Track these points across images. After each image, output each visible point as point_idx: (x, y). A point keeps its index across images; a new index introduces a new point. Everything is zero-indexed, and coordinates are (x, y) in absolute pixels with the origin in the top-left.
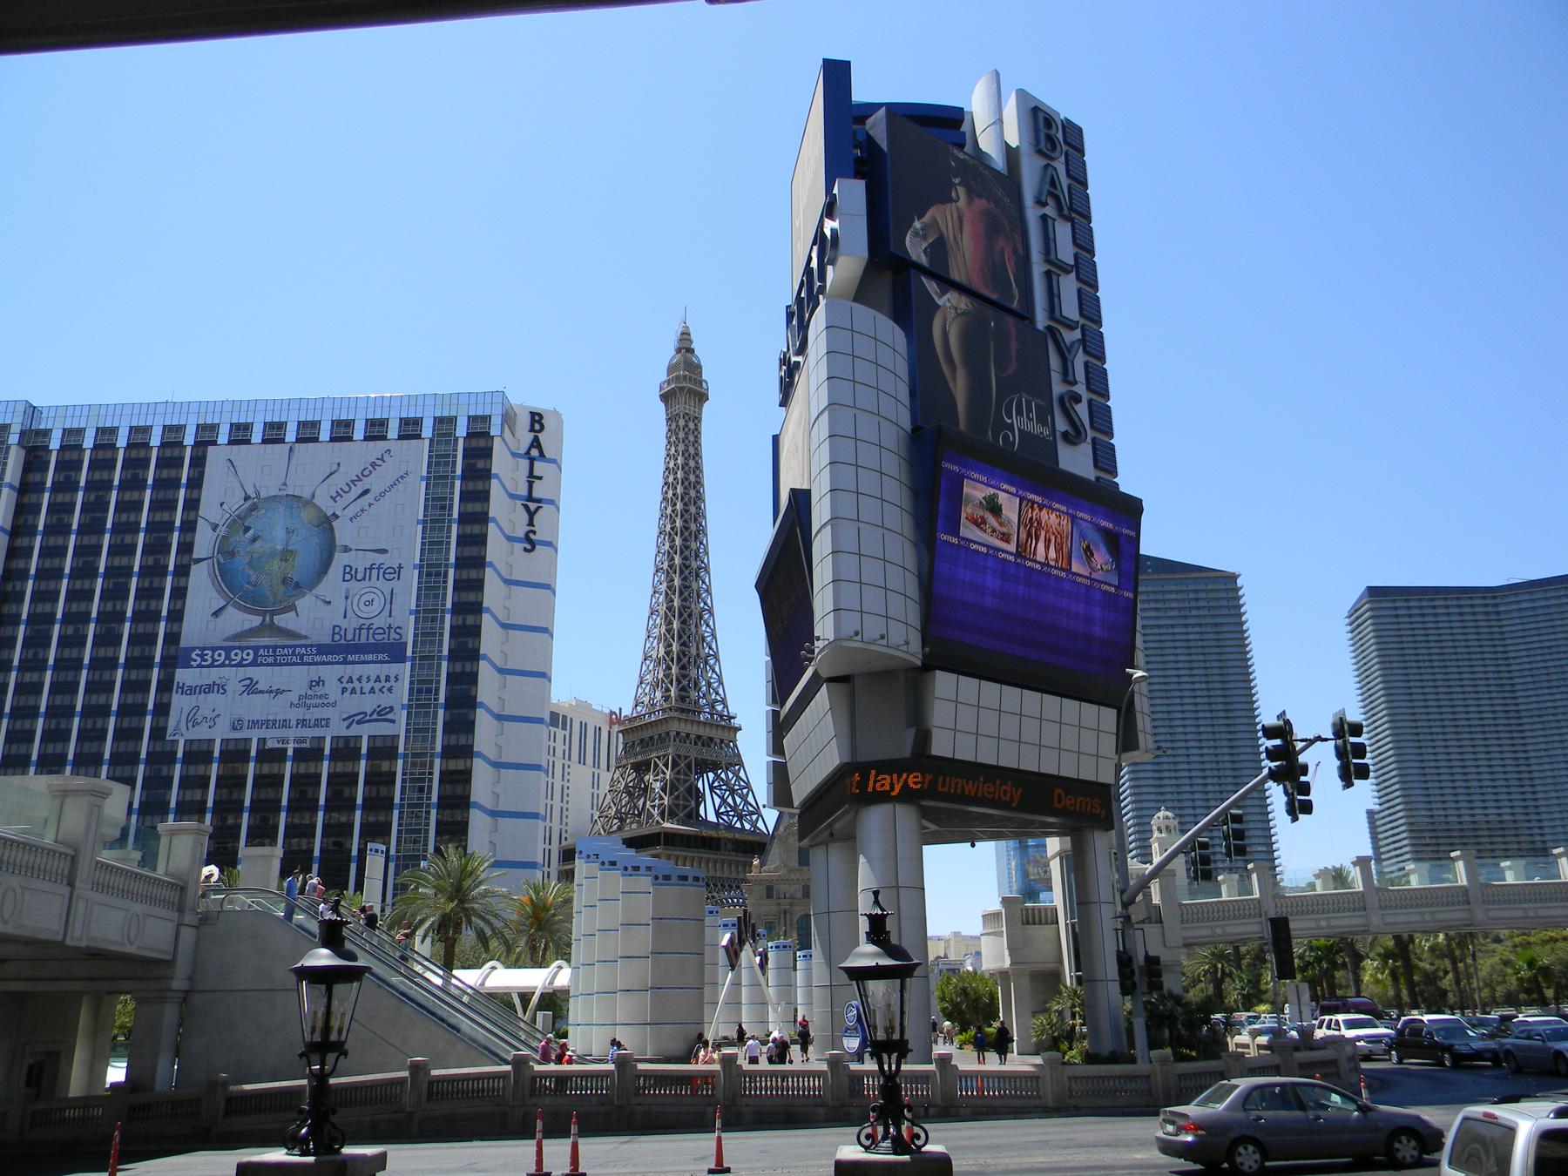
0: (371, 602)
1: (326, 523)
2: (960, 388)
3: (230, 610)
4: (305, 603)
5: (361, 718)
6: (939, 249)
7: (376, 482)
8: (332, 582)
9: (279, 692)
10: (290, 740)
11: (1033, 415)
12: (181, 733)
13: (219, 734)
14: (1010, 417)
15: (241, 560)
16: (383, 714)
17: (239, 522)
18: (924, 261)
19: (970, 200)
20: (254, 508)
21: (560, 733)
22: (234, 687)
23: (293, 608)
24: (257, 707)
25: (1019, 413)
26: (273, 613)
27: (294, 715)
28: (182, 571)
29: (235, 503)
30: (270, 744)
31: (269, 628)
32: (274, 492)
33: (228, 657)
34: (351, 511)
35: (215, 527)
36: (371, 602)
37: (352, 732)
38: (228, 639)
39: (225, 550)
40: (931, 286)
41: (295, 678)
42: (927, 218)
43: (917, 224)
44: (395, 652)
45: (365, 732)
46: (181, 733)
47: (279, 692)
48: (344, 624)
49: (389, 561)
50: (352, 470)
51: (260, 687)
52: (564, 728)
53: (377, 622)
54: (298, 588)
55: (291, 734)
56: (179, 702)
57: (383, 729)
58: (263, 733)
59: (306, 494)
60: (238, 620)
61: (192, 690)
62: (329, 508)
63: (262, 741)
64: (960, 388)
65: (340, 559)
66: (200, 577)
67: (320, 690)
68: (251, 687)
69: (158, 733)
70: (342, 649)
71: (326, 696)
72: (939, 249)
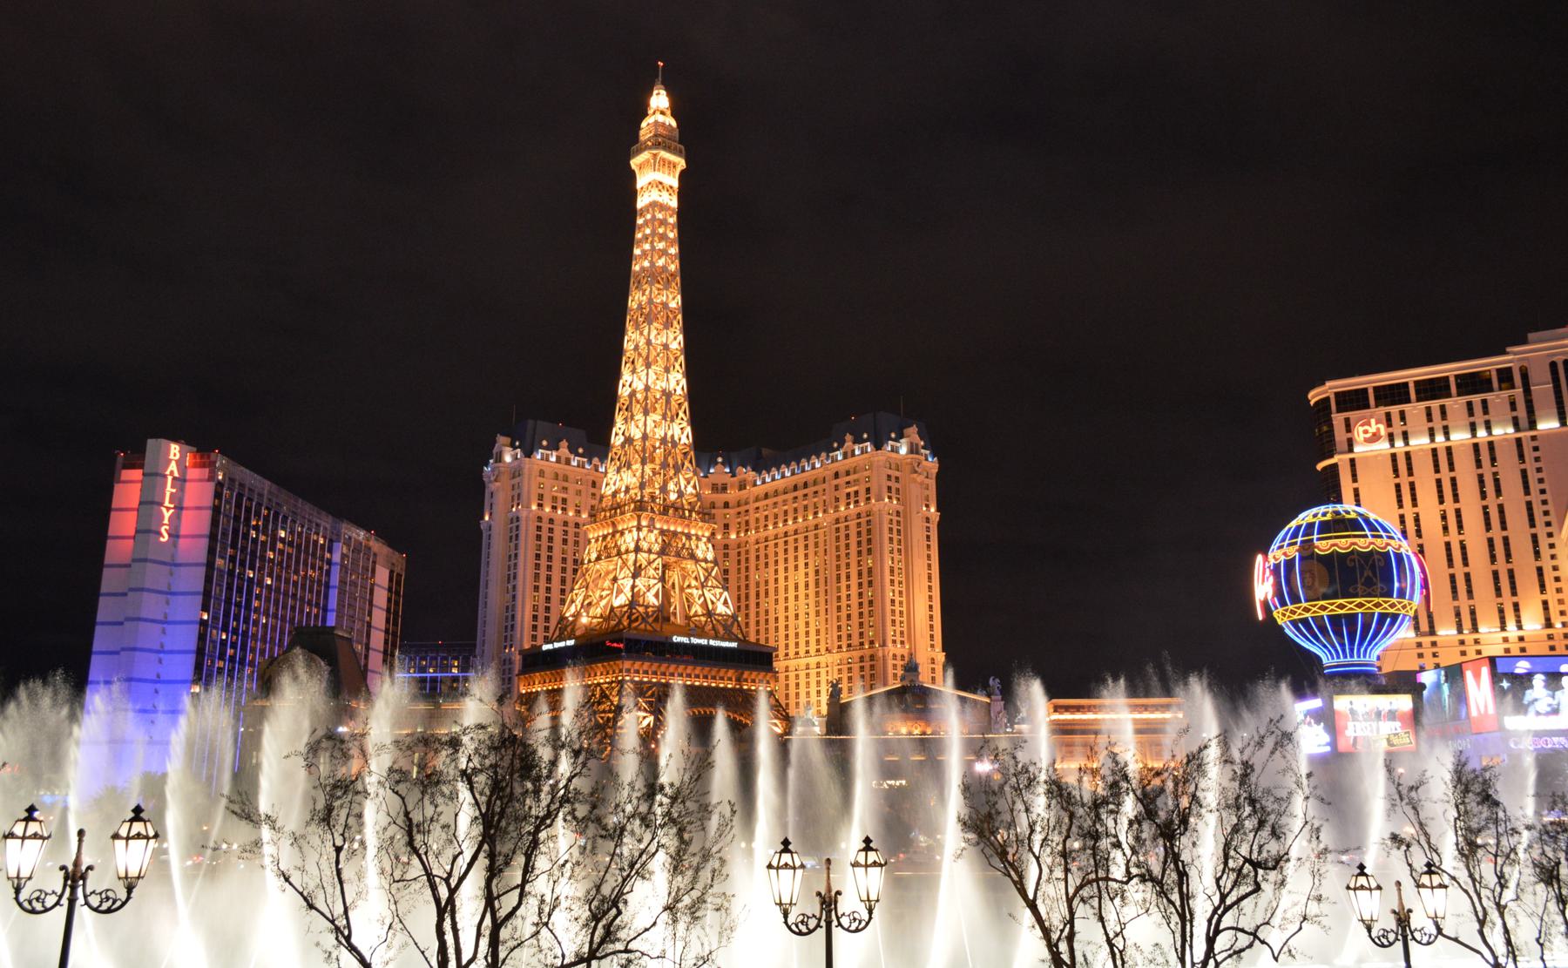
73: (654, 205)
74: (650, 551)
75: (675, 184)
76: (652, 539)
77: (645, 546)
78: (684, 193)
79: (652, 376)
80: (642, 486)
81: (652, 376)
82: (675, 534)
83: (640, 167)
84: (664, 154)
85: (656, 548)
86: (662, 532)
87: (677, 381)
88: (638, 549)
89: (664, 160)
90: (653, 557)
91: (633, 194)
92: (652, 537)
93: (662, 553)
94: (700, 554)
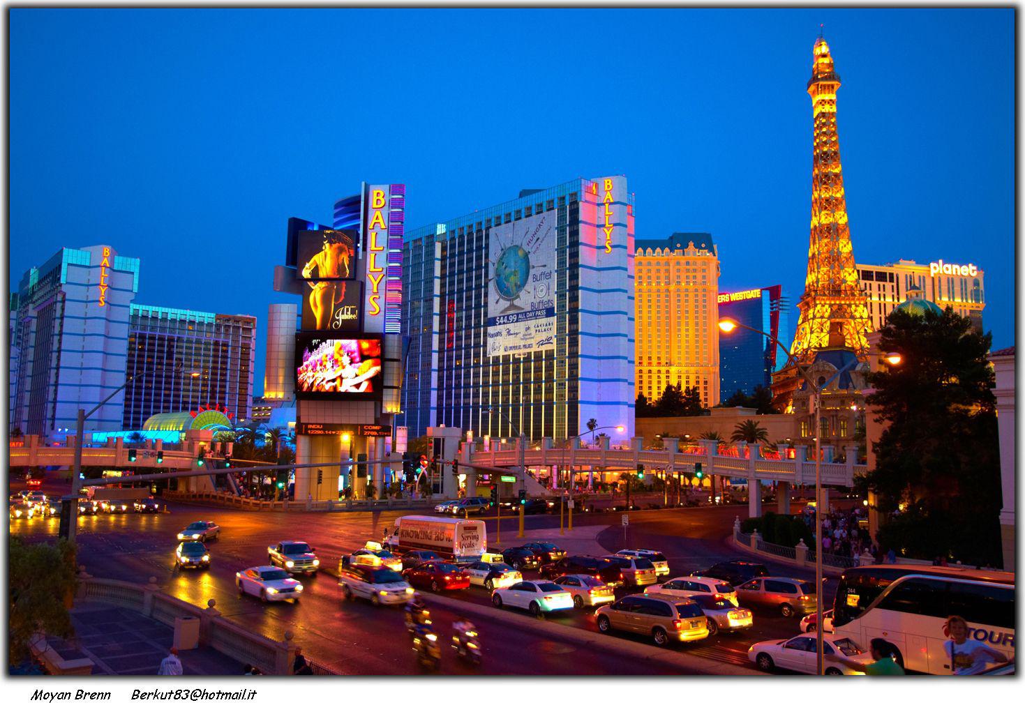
0: (542, 291)
1: (526, 255)
2: (318, 314)
3: (501, 300)
4: (522, 293)
5: (541, 343)
6: (316, 270)
7: (540, 234)
8: (530, 286)
9: (517, 334)
10: (520, 353)
11: (349, 313)
12: (491, 354)
13: (501, 353)
14: (338, 316)
15: (503, 277)
16: (549, 341)
17: (501, 261)
18: (309, 276)
19: (331, 246)
20: (504, 254)
21: (888, 285)
22: (504, 333)
23: (518, 297)
24: (511, 341)
25: (343, 313)
26: (513, 299)
27: (522, 343)
28: (486, 286)
29: (500, 253)
30: (516, 356)
31: (512, 306)
32: (510, 245)
33: (508, 319)
34: (533, 250)
35: (494, 264)
36: (542, 291)
37: (539, 350)
38: (502, 312)
39: (498, 275)
40: (311, 284)
41: (519, 327)
42: (312, 261)
43: (307, 265)
44: (550, 312)
45: (544, 348)
46: (491, 354)
47: (517, 334)
48: (533, 300)
49: (546, 270)
50: (532, 230)
51: (511, 332)
52: (892, 280)
53: (545, 299)
54: (520, 287)
55: (522, 351)
56: (490, 341)
57: (549, 347)
58: (516, 352)
59: (519, 245)
60: (504, 304)
61: (492, 336)
62: (527, 249)
63: (514, 355)
64: (318, 314)
65: (532, 272)
66: (491, 286)
67: (529, 332)
68: (509, 333)
69: (485, 353)
70: (533, 313)
71: (530, 334)
72: (316, 270)
73: (823, 115)
74: (822, 317)
75: (833, 97)
76: (827, 311)
77: (818, 315)
78: (838, 103)
79: (823, 217)
80: (817, 282)
81: (823, 217)
82: (840, 305)
83: (814, 93)
84: (821, 83)
85: (827, 315)
86: (831, 305)
87: (842, 218)
88: (814, 317)
89: (825, 85)
90: (824, 320)
91: (812, 109)
92: (824, 309)
93: (829, 318)
94: (857, 315)
